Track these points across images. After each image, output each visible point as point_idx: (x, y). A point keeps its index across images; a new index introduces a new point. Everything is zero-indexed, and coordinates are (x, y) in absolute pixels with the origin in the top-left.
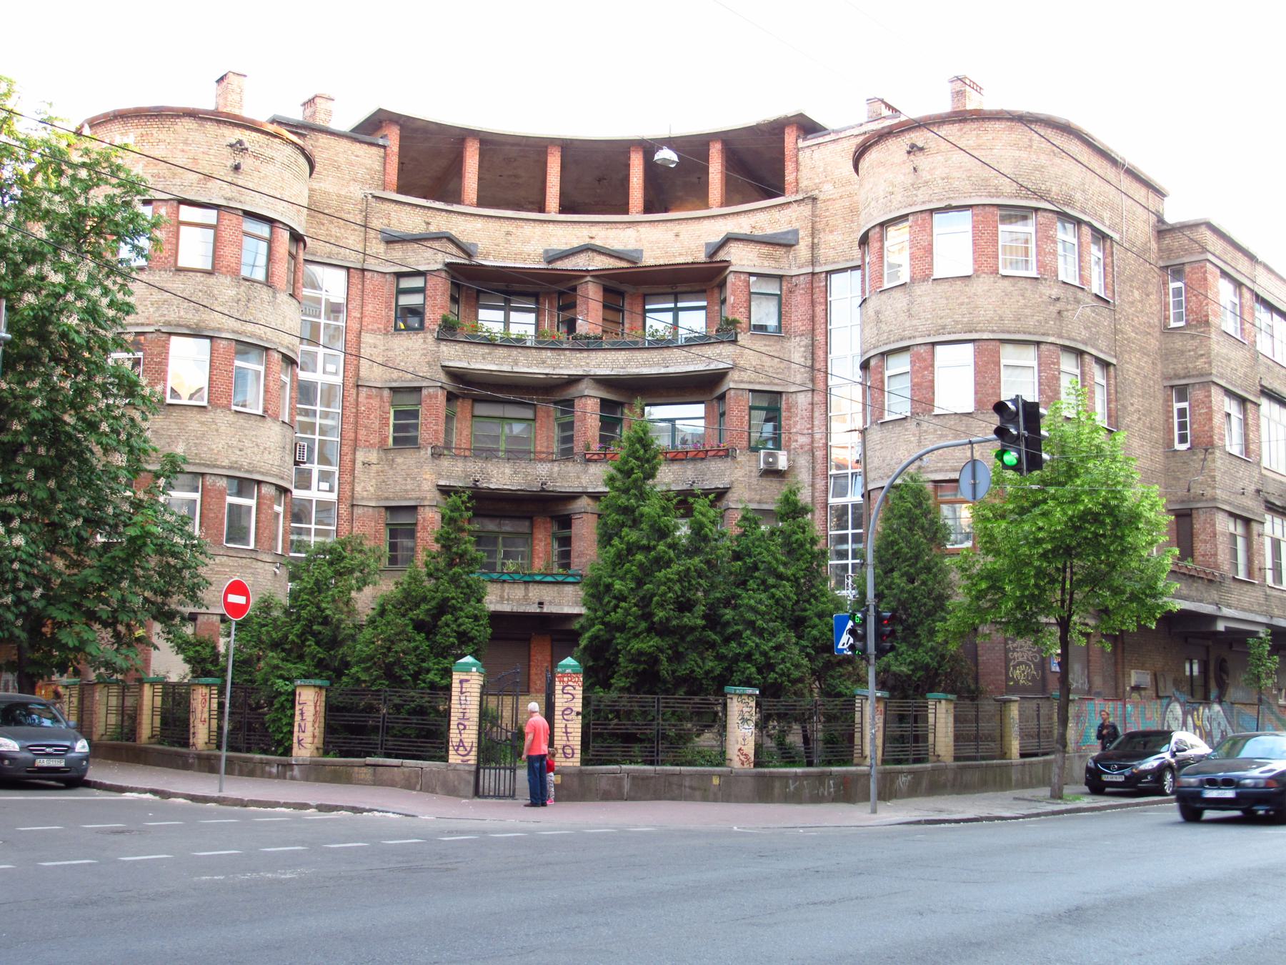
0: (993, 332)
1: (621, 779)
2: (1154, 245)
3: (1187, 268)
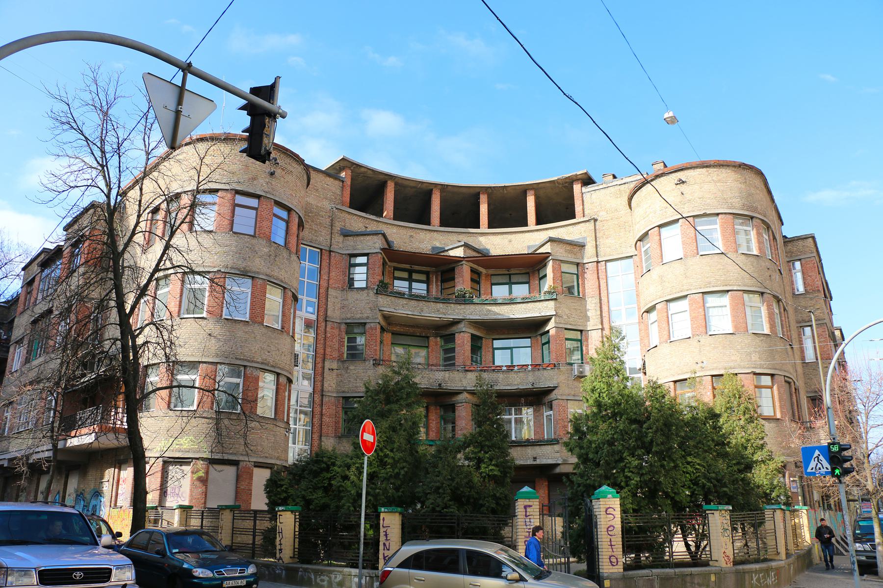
1: (653, 580)
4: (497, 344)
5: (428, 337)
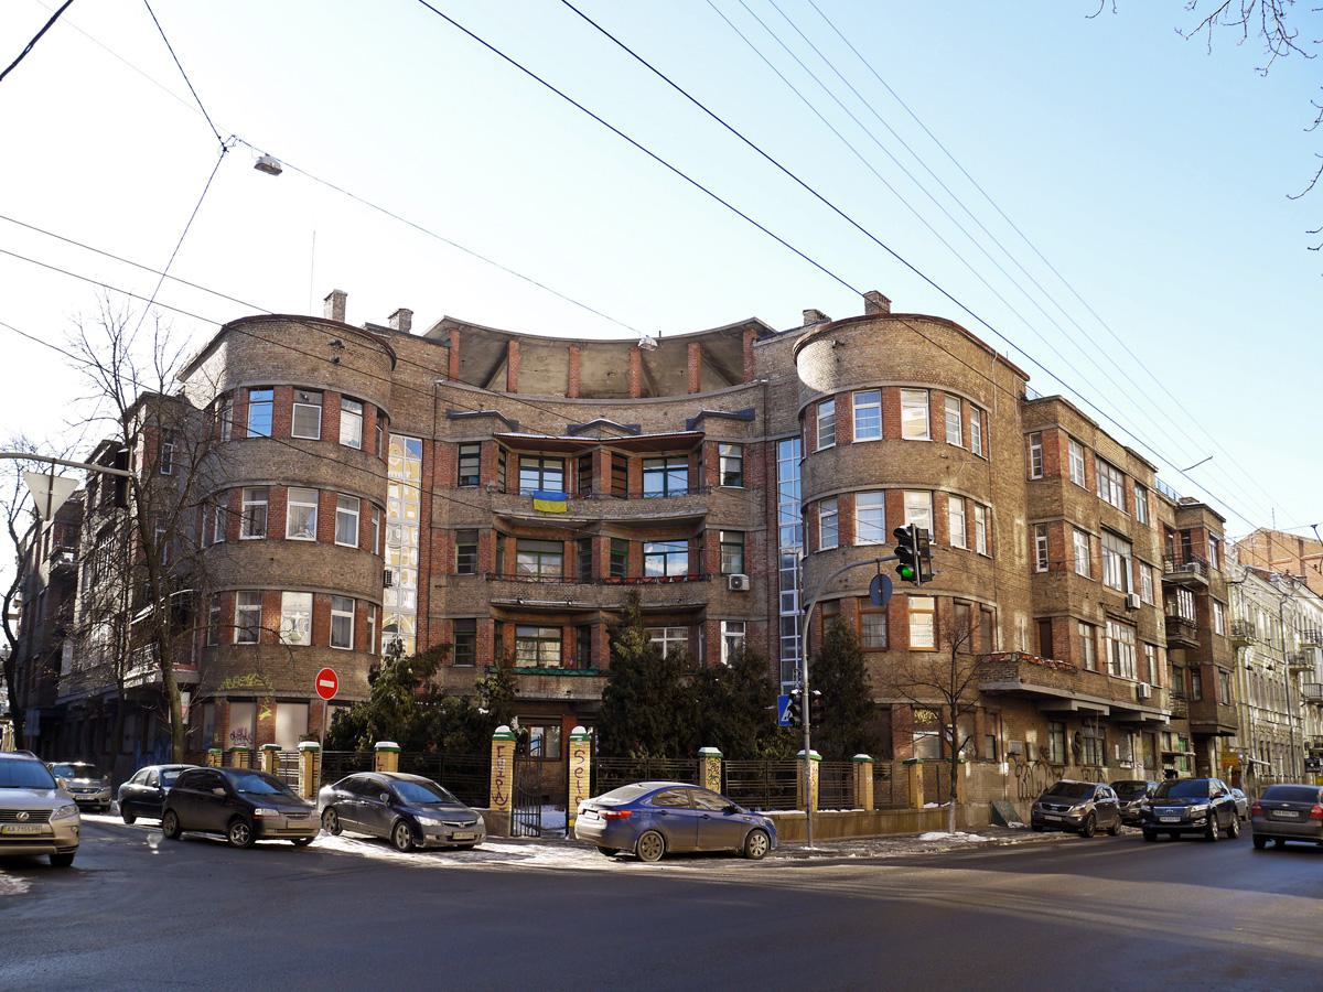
0: (899, 483)
2: (1018, 417)
3: (1044, 435)
4: (649, 549)
5: (563, 542)
